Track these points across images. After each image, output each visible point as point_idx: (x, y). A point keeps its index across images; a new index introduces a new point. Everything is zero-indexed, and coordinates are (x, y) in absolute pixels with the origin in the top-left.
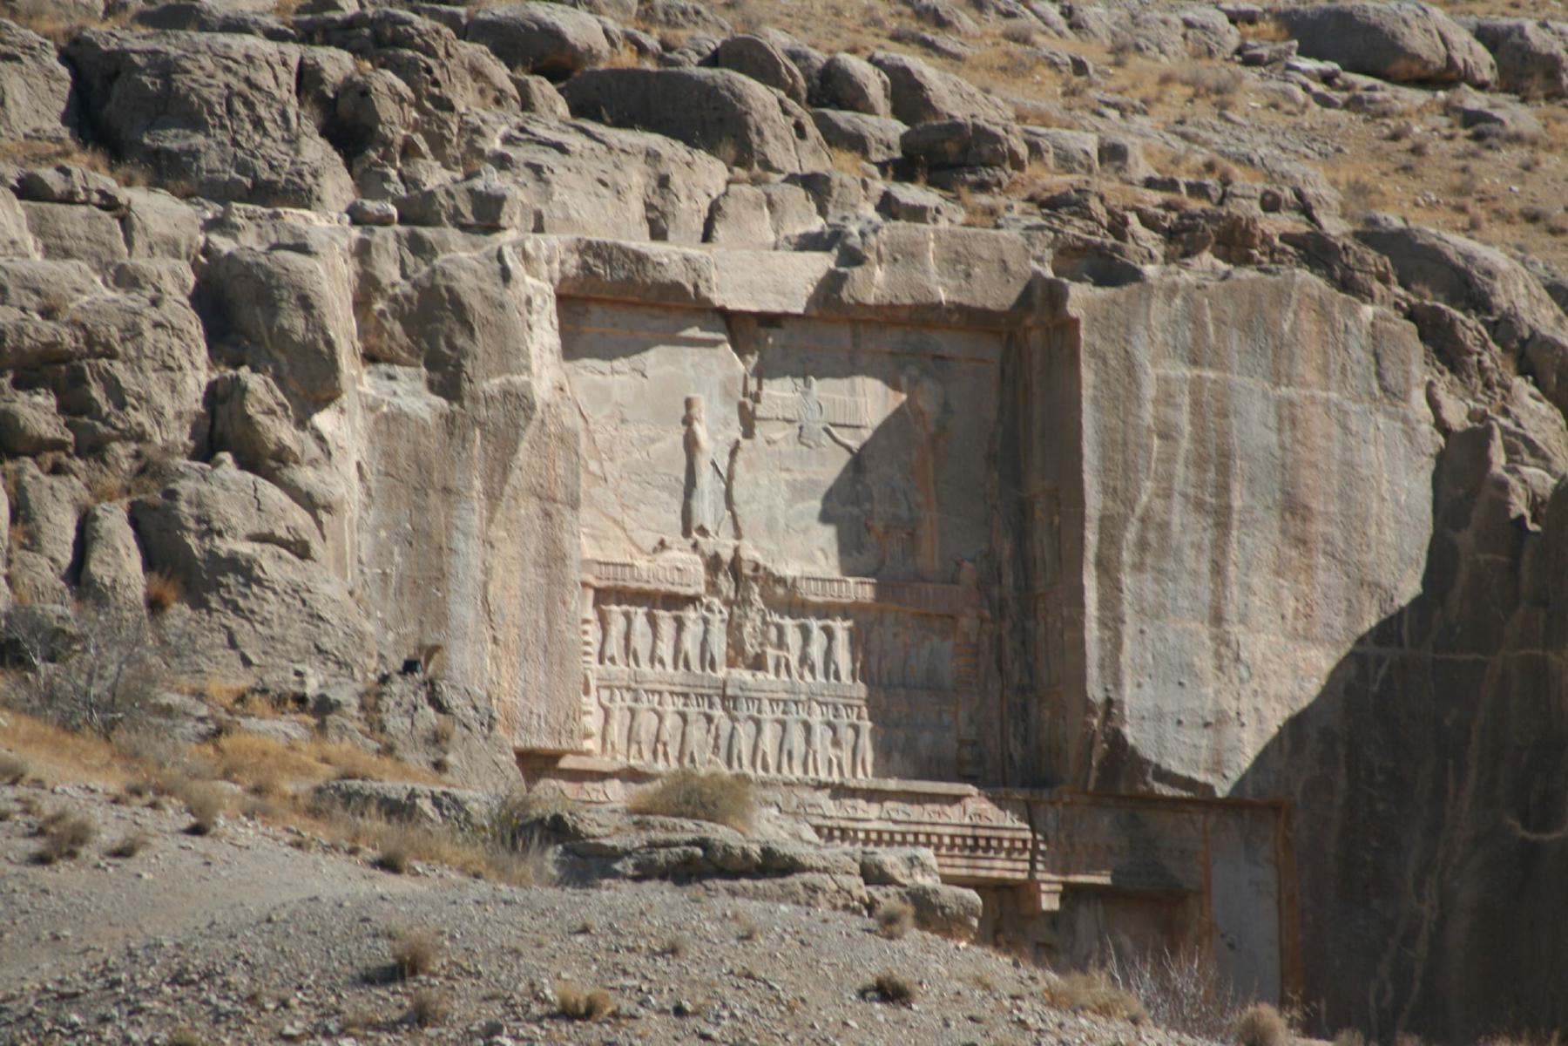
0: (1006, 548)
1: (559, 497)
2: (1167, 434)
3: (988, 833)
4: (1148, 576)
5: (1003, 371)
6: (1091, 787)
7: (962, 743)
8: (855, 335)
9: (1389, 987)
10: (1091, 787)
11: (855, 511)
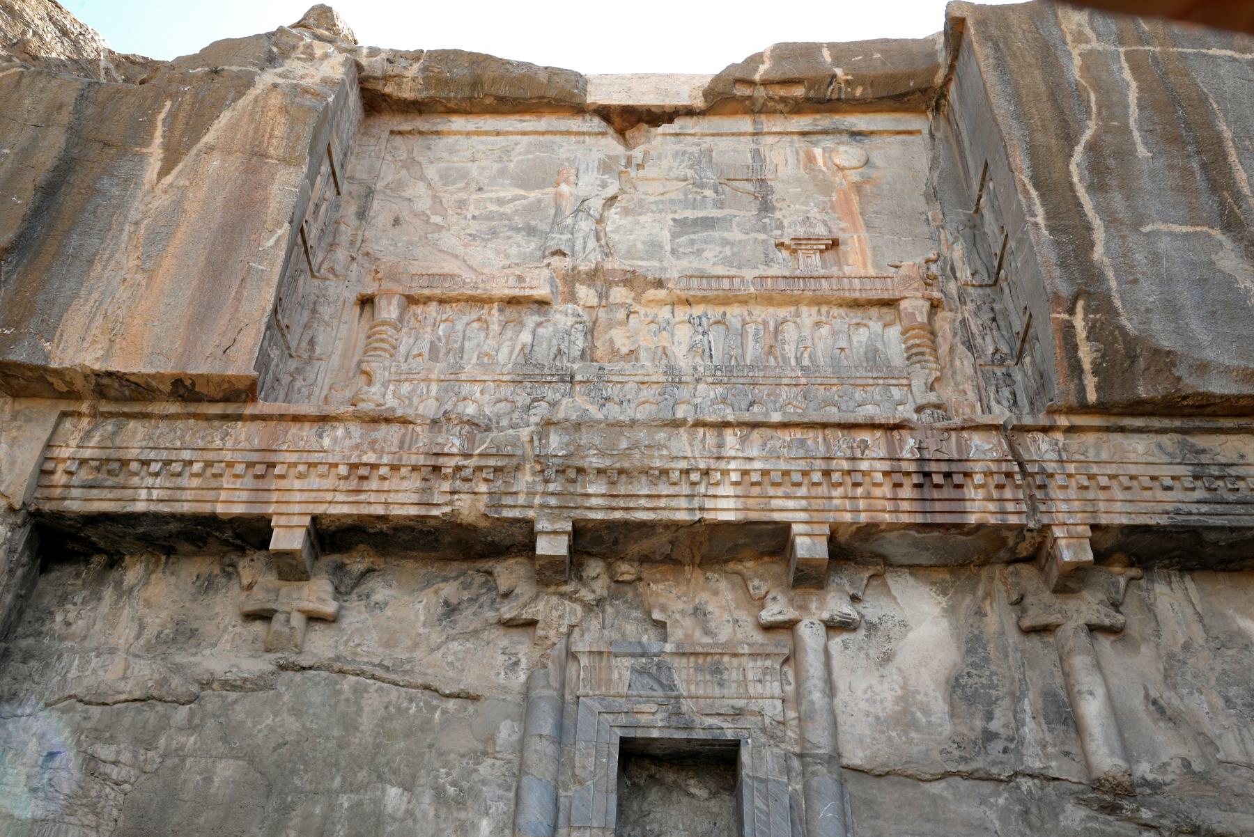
1: (272, 151)
3: (944, 467)
5: (932, 136)
6: (1092, 397)
8: (755, 122)
10: (1092, 397)
11: (763, 237)
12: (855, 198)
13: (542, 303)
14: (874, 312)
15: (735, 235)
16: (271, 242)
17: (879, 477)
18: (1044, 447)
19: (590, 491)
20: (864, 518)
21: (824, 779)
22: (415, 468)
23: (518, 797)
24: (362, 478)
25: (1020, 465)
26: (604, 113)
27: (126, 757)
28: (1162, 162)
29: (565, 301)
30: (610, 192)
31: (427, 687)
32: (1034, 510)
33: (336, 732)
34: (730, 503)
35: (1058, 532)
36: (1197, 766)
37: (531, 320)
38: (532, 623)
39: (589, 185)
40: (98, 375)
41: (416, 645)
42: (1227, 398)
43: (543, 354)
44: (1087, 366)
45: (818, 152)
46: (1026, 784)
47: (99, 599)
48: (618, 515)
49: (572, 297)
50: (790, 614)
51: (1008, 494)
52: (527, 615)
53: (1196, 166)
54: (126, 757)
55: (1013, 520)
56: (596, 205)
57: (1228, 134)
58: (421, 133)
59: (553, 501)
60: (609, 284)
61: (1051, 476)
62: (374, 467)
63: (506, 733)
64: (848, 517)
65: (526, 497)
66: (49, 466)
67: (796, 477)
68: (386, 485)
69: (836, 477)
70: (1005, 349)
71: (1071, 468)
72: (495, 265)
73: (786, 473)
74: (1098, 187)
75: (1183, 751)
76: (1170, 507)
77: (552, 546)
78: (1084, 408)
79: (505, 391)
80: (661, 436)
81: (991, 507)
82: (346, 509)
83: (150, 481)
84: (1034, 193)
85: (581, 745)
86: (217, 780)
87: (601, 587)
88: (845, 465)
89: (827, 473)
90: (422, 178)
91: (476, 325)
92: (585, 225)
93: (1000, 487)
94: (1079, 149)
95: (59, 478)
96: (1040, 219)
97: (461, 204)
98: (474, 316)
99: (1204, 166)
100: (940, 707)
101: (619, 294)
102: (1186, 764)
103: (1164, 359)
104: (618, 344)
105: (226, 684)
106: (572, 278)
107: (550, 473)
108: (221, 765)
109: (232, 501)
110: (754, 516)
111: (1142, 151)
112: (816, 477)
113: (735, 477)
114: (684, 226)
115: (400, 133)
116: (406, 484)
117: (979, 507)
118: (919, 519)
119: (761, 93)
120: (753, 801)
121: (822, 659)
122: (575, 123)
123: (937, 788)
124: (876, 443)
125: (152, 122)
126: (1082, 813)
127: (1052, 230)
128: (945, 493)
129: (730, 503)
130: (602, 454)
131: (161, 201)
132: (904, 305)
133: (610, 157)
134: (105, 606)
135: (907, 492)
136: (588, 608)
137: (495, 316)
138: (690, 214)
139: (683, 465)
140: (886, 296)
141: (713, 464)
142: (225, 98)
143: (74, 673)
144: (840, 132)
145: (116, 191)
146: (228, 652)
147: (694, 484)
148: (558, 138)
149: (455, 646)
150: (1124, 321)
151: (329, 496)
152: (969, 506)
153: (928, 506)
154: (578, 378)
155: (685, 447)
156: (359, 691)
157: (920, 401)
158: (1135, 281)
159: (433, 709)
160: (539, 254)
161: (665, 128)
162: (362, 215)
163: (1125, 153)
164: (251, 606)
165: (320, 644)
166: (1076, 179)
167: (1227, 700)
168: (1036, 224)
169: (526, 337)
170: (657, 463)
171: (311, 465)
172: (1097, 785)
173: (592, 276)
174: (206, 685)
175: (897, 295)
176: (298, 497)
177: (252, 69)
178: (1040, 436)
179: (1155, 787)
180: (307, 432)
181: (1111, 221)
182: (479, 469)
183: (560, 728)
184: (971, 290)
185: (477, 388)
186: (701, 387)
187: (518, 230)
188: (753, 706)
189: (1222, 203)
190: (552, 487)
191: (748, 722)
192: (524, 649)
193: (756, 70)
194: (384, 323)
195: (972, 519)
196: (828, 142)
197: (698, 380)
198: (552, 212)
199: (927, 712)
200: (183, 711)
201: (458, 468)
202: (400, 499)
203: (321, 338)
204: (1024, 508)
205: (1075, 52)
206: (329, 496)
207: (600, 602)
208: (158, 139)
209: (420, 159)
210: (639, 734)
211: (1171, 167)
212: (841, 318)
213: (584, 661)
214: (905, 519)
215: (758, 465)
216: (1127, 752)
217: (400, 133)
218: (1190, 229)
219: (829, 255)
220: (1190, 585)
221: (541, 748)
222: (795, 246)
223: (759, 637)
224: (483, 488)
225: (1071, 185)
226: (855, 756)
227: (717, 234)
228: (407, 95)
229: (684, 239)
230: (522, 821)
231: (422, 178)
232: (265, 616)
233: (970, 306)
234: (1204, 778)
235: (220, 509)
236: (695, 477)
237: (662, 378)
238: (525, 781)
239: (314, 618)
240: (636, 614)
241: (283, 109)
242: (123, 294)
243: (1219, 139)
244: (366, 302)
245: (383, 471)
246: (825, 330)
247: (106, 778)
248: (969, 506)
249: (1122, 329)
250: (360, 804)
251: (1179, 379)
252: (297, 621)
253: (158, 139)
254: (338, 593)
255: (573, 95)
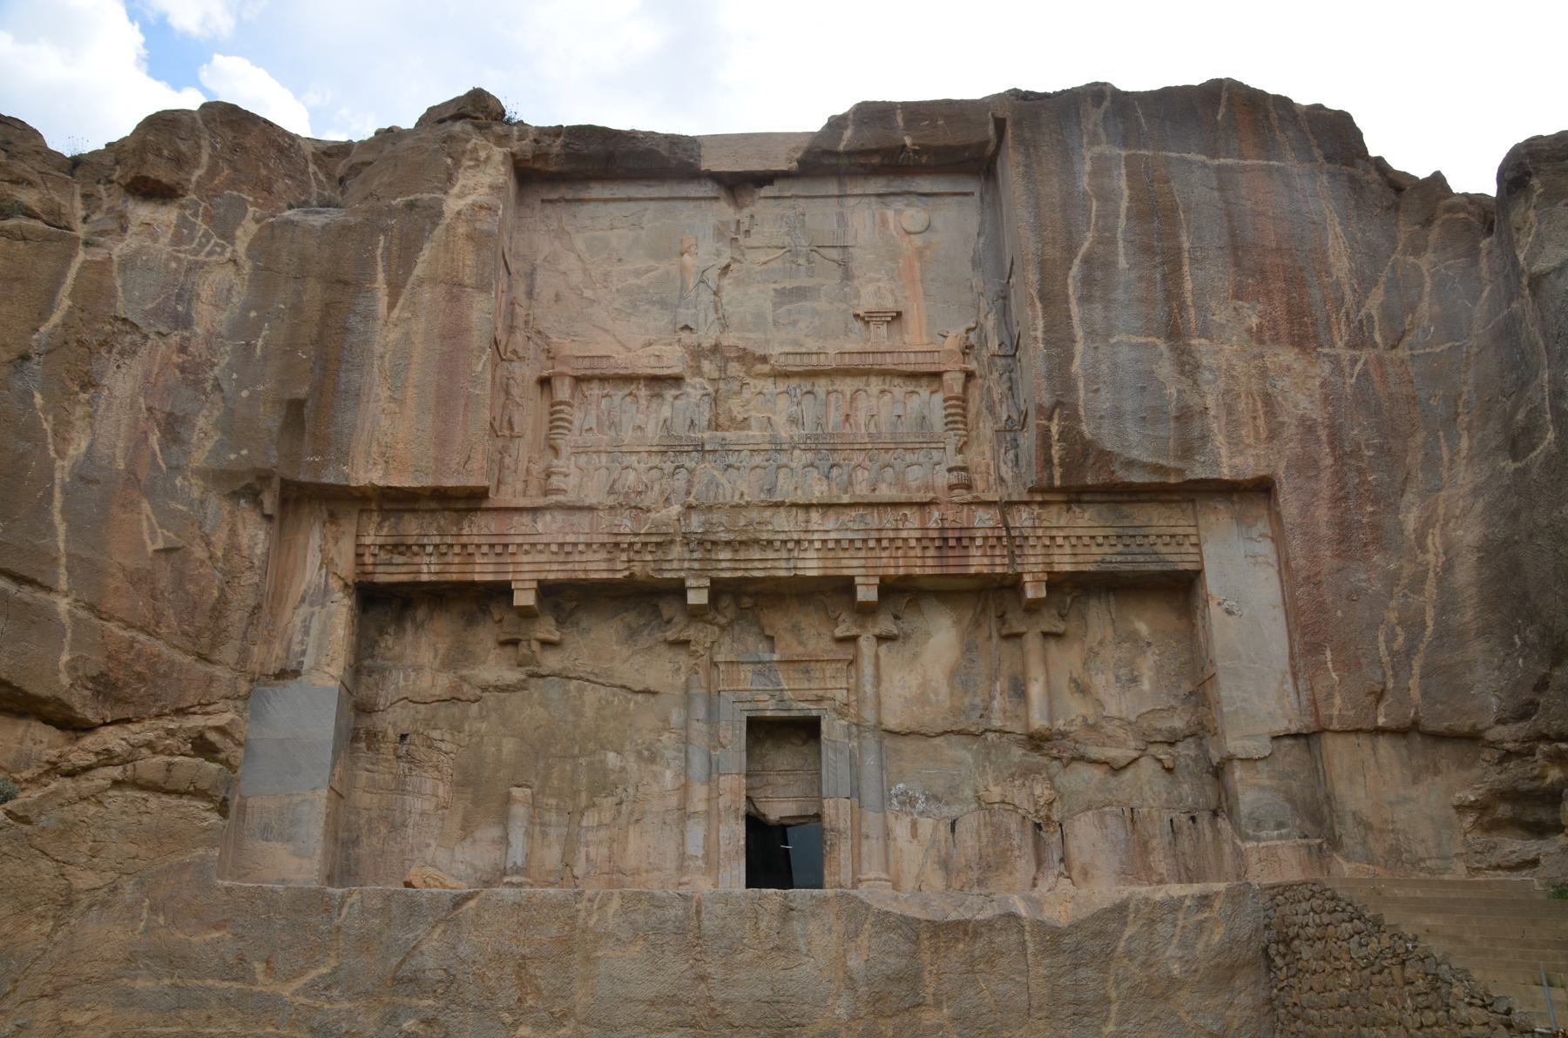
0: (990, 323)
1: (467, 281)
2: (1106, 196)
3: (957, 534)
4: (1098, 306)
6: (1057, 483)
7: (950, 470)
9: (1398, 629)
11: (843, 306)
12: (917, 265)
13: (677, 380)
14: (924, 382)
15: (822, 304)
16: (479, 369)
17: (913, 543)
18: (1025, 515)
19: (721, 557)
20: (902, 571)
21: (870, 741)
22: (603, 545)
23: (687, 759)
24: (568, 553)
25: (1008, 529)
26: (717, 178)
27: (447, 737)
28: (1133, 275)
29: (694, 375)
30: (724, 262)
31: (623, 687)
32: (1013, 562)
33: (571, 718)
34: (814, 564)
35: (1027, 578)
36: (1091, 721)
37: (670, 393)
38: (687, 643)
39: (705, 254)
40: (382, 488)
41: (613, 659)
42: (1143, 484)
43: (680, 429)
44: (1056, 461)
45: (890, 214)
46: (990, 736)
47: (404, 631)
48: (739, 574)
49: (698, 371)
50: (854, 631)
51: (997, 552)
52: (683, 636)
53: (1158, 276)
54: (447, 737)
55: (999, 570)
56: (713, 274)
57: (1186, 245)
58: (567, 201)
59: (696, 565)
60: (727, 360)
61: (1027, 538)
62: (575, 544)
63: (676, 717)
64: (892, 571)
65: (676, 564)
66: (361, 551)
67: (858, 544)
68: (584, 558)
69: (885, 543)
70: (1015, 417)
71: (1040, 532)
72: (639, 342)
73: (852, 541)
74: (1085, 299)
75: (1084, 711)
76: (1099, 558)
77: (697, 598)
78: (1051, 489)
79: (656, 460)
80: (768, 513)
81: (986, 561)
82: (561, 576)
83: (426, 559)
84: (1039, 305)
85: (723, 723)
86: (505, 751)
87: (730, 613)
88: (891, 534)
89: (879, 540)
90: (572, 249)
91: (629, 399)
92: (706, 297)
93: (993, 547)
94: (1077, 261)
95: (368, 559)
96: (1040, 334)
97: (606, 275)
98: (627, 391)
99: (1164, 277)
100: (944, 690)
101: (734, 368)
102: (1085, 719)
103: (1105, 457)
104: (735, 413)
105: (496, 688)
106: (697, 353)
107: (692, 546)
108: (505, 741)
109: (483, 571)
110: (831, 572)
111: (1122, 262)
112: (872, 544)
113: (817, 545)
114: (786, 296)
115: (550, 201)
116: (598, 556)
117: (978, 563)
118: (938, 571)
119: (844, 161)
120: (828, 754)
121: (873, 660)
122: (693, 190)
123: (938, 741)
124: (913, 518)
125: (374, 257)
126: (1020, 752)
127: (1048, 343)
128: (957, 553)
129: (814, 564)
130: (728, 531)
131: (394, 335)
132: (946, 377)
133: (722, 223)
134: (409, 637)
135: (931, 552)
136: (723, 628)
137: (643, 392)
138: (789, 284)
139: (783, 536)
140: (933, 369)
141: (803, 536)
142: (423, 230)
143: (402, 683)
144: (910, 193)
145: (361, 327)
146: (495, 668)
147: (790, 550)
148: (680, 204)
149: (639, 659)
150: (1084, 427)
151: (547, 567)
152: (972, 561)
153: (945, 562)
154: (707, 448)
155: (784, 523)
156: (581, 691)
157: (953, 465)
158: (1097, 391)
159: (628, 701)
160: (671, 327)
161: (767, 191)
162: (530, 294)
163: (1109, 265)
164: (503, 638)
165: (552, 661)
166: (1071, 291)
167: (1117, 677)
168: (1035, 338)
169: (666, 412)
170: (765, 536)
171: (533, 545)
172: (1031, 737)
173: (716, 349)
174: (484, 689)
175: (942, 368)
176: (527, 568)
177: (439, 195)
178: (1022, 508)
179: (1064, 735)
180: (526, 519)
181: (1091, 333)
182: (645, 544)
183: (710, 713)
184: (997, 360)
185: (634, 458)
186: (797, 452)
187: (653, 303)
188: (829, 694)
189: (1170, 314)
190: (696, 555)
191: (826, 704)
192: (682, 658)
193: (840, 139)
194: (561, 403)
195: (972, 570)
196: (899, 203)
197: (794, 448)
198: (679, 283)
199: (936, 693)
200: (475, 707)
201: (631, 544)
202: (596, 567)
203: (516, 419)
204: (1006, 561)
205: (1088, 155)
206: (547, 567)
207: (731, 624)
208: (381, 276)
209: (568, 228)
210: (759, 714)
211: (1141, 279)
212: (899, 389)
213: (722, 667)
214: (929, 571)
215: (833, 536)
216: (1051, 716)
217: (550, 201)
218: (1143, 340)
219: (895, 326)
220: (1112, 600)
221: (699, 728)
222: (865, 319)
223: (833, 646)
224: (649, 557)
225: (1067, 296)
226: (891, 723)
227: (808, 304)
228: (553, 168)
229: (784, 309)
230: (690, 773)
231: (572, 249)
232: (515, 643)
233: (996, 375)
234: (1093, 727)
235: (477, 578)
236: (790, 545)
237: (767, 447)
238: (690, 748)
239: (545, 644)
240: (755, 629)
241: (469, 237)
242: (385, 422)
243: (1179, 250)
244: (545, 382)
245: (581, 547)
246: (887, 397)
247: (439, 750)
248: (972, 561)
249: (1081, 433)
250: (591, 763)
251: (1113, 473)
252: (535, 646)
253: (381, 276)
254: (560, 623)
255: (691, 165)
